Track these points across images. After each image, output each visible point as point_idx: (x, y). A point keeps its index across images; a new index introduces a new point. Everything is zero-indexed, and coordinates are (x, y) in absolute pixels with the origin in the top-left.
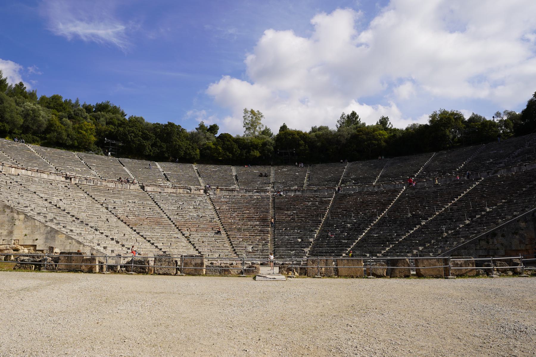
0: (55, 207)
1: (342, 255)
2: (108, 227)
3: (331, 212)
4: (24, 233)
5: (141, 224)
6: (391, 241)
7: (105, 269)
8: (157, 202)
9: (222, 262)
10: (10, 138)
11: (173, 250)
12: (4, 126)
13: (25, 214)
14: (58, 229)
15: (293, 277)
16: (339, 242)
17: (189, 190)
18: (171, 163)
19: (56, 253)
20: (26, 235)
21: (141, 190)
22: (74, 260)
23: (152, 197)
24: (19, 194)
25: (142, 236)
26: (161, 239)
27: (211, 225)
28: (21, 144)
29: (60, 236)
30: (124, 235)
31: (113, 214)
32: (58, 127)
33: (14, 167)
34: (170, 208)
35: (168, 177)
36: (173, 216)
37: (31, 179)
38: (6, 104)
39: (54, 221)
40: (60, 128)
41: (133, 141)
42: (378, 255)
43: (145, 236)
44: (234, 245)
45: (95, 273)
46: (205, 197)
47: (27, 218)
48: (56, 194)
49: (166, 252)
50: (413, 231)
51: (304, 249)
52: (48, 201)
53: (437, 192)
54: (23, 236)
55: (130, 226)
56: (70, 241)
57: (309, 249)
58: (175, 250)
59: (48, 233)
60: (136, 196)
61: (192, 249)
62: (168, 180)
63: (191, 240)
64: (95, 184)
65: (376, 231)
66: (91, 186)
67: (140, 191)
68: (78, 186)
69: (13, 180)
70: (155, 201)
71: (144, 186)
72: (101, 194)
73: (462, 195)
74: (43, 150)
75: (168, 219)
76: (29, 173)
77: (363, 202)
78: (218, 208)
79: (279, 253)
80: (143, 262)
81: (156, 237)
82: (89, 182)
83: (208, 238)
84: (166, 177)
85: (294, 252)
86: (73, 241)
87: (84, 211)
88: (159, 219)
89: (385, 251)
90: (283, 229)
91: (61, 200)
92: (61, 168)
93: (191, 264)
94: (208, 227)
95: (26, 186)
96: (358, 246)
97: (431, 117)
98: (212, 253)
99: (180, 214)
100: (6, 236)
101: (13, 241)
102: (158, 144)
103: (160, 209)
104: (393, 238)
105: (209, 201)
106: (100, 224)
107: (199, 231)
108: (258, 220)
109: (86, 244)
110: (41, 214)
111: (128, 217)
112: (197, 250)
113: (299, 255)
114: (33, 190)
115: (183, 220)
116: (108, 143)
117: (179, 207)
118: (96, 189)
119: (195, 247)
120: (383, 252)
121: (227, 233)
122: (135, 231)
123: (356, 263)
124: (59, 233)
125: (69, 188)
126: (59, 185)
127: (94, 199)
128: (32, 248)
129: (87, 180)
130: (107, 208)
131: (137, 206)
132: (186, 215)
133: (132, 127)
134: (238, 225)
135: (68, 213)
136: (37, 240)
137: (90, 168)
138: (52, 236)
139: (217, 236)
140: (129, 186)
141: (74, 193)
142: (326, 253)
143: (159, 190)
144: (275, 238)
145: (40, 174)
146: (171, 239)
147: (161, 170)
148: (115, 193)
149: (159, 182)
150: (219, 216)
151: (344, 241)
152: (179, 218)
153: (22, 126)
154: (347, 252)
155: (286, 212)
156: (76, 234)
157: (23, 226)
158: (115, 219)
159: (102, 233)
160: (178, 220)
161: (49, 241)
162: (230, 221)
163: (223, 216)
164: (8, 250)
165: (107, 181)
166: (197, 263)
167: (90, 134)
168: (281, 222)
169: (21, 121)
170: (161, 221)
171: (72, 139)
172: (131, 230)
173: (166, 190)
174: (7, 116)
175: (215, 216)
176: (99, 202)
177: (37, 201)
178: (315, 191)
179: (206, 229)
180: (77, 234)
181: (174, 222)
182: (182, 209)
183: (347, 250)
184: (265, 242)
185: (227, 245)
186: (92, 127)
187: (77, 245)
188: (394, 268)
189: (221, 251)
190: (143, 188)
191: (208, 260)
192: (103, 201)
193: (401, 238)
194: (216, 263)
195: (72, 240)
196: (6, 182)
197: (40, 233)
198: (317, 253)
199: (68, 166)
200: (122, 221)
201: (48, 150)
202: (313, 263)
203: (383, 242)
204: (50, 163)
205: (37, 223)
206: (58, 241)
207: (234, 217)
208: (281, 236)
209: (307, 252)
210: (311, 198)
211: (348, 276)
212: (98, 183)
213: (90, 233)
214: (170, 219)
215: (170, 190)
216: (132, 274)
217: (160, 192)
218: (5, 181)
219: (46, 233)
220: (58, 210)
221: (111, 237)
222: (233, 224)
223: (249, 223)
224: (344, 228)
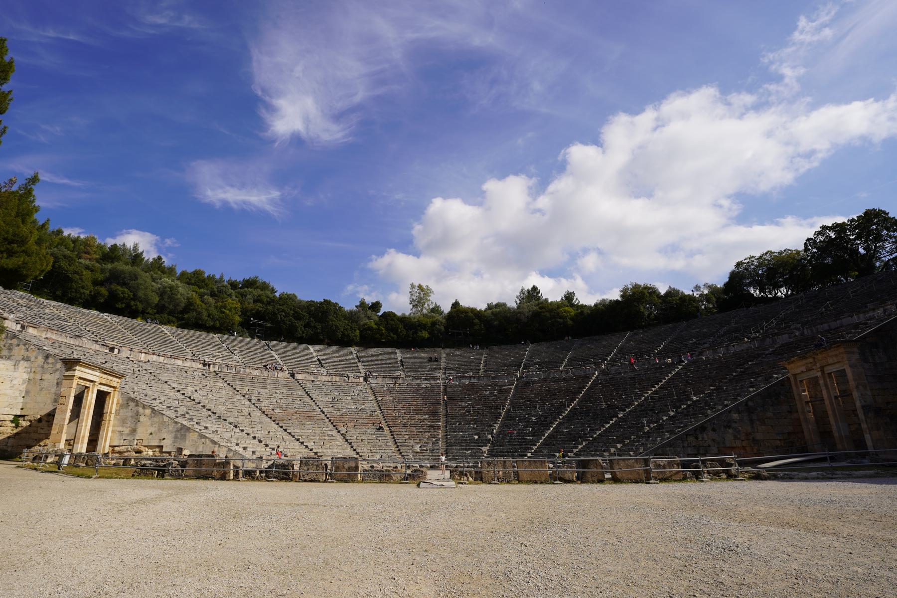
0: (189, 399)
2: (250, 423)
3: (512, 402)
4: (149, 431)
5: (290, 419)
6: (584, 437)
7: (240, 475)
8: (309, 393)
9: (384, 465)
10: (143, 319)
11: (326, 450)
12: (137, 305)
13: (152, 408)
14: (190, 427)
15: (465, 483)
18: (326, 346)
19: (185, 455)
20: (151, 434)
21: (291, 378)
22: (204, 464)
23: (303, 387)
24: (147, 384)
25: (290, 433)
26: (312, 438)
28: (154, 325)
30: (269, 432)
31: (257, 407)
32: (198, 305)
33: (144, 353)
34: (323, 399)
35: (323, 362)
36: (327, 409)
37: (163, 367)
39: (187, 416)
40: (200, 307)
41: (283, 321)
43: (293, 434)
45: (229, 480)
46: (365, 386)
47: (154, 413)
48: (191, 384)
50: (609, 425)
51: (482, 448)
52: (181, 392)
53: (634, 378)
54: (148, 435)
55: (277, 422)
56: (203, 440)
57: (488, 448)
58: (328, 450)
59: (178, 431)
60: (284, 386)
62: (322, 366)
63: (347, 438)
65: (566, 425)
68: (217, 374)
69: (142, 367)
70: (307, 391)
71: (294, 374)
72: (243, 384)
74: (179, 332)
75: (321, 413)
76: (161, 359)
77: (549, 391)
78: (380, 399)
79: (452, 453)
80: (287, 466)
81: (307, 434)
83: (368, 435)
84: (320, 362)
85: (469, 452)
86: (207, 440)
89: (577, 450)
91: (196, 391)
93: (344, 467)
95: (155, 374)
96: (546, 444)
98: (373, 454)
99: (336, 407)
100: (128, 435)
101: (136, 441)
103: (312, 401)
104: (586, 434)
105: (369, 391)
106: (241, 419)
107: (358, 427)
108: (427, 413)
109: (222, 444)
110: (172, 408)
111: (275, 411)
112: (355, 450)
113: (476, 456)
114: (164, 379)
115: (339, 414)
117: (335, 398)
118: (237, 377)
119: (352, 447)
120: (575, 451)
121: (390, 429)
122: (282, 427)
123: (539, 465)
125: (206, 377)
126: (195, 373)
127: (235, 389)
128: (157, 450)
129: (228, 366)
130: (250, 400)
131: (286, 398)
132: (342, 407)
133: (283, 305)
135: (204, 406)
136: (164, 439)
137: (233, 353)
140: (276, 374)
141: (212, 382)
142: (507, 452)
144: (447, 435)
146: (324, 437)
147: (315, 354)
148: (261, 382)
149: (312, 369)
150: (382, 408)
151: (528, 438)
153: (157, 305)
154: (533, 451)
155: (460, 403)
156: (211, 432)
157: (149, 423)
158: (259, 413)
159: (242, 431)
161: (179, 440)
162: (394, 414)
163: (386, 408)
164: (129, 452)
166: (351, 467)
167: (234, 314)
169: (156, 299)
170: (312, 415)
172: (276, 426)
173: (320, 378)
175: (377, 408)
176: (240, 393)
177: (167, 392)
178: (494, 378)
179: (365, 425)
180: (213, 431)
181: (328, 416)
182: (337, 400)
183: (532, 449)
184: (436, 440)
185: (391, 443)
187: (211, 445)
188: (584, 471)
189: (383, 451)
190: (293, 375)
191: (368, 463)
192: (245, 392)
193: (596, 433)
196: (134, 370)
197: (168, 431)
198: (497, 452)
199: (207, 351)
200: (267, 415)
201: (185, 332)
202: (489, 465)
203: (574, 438)
204: (186, 347)
205: (166, 419)
208: (454, 432)
209: (485, 452)
210: (489, 386)
211: (531, 481)
213: (228, 430)
214: (324, 413)
215: (324, 378)
216: (272, 481)
217: (313, 381)
218: (132, 369)
219: (176, 431)
220: (192, 403)
223: (417, 416)
224: (528, 421)
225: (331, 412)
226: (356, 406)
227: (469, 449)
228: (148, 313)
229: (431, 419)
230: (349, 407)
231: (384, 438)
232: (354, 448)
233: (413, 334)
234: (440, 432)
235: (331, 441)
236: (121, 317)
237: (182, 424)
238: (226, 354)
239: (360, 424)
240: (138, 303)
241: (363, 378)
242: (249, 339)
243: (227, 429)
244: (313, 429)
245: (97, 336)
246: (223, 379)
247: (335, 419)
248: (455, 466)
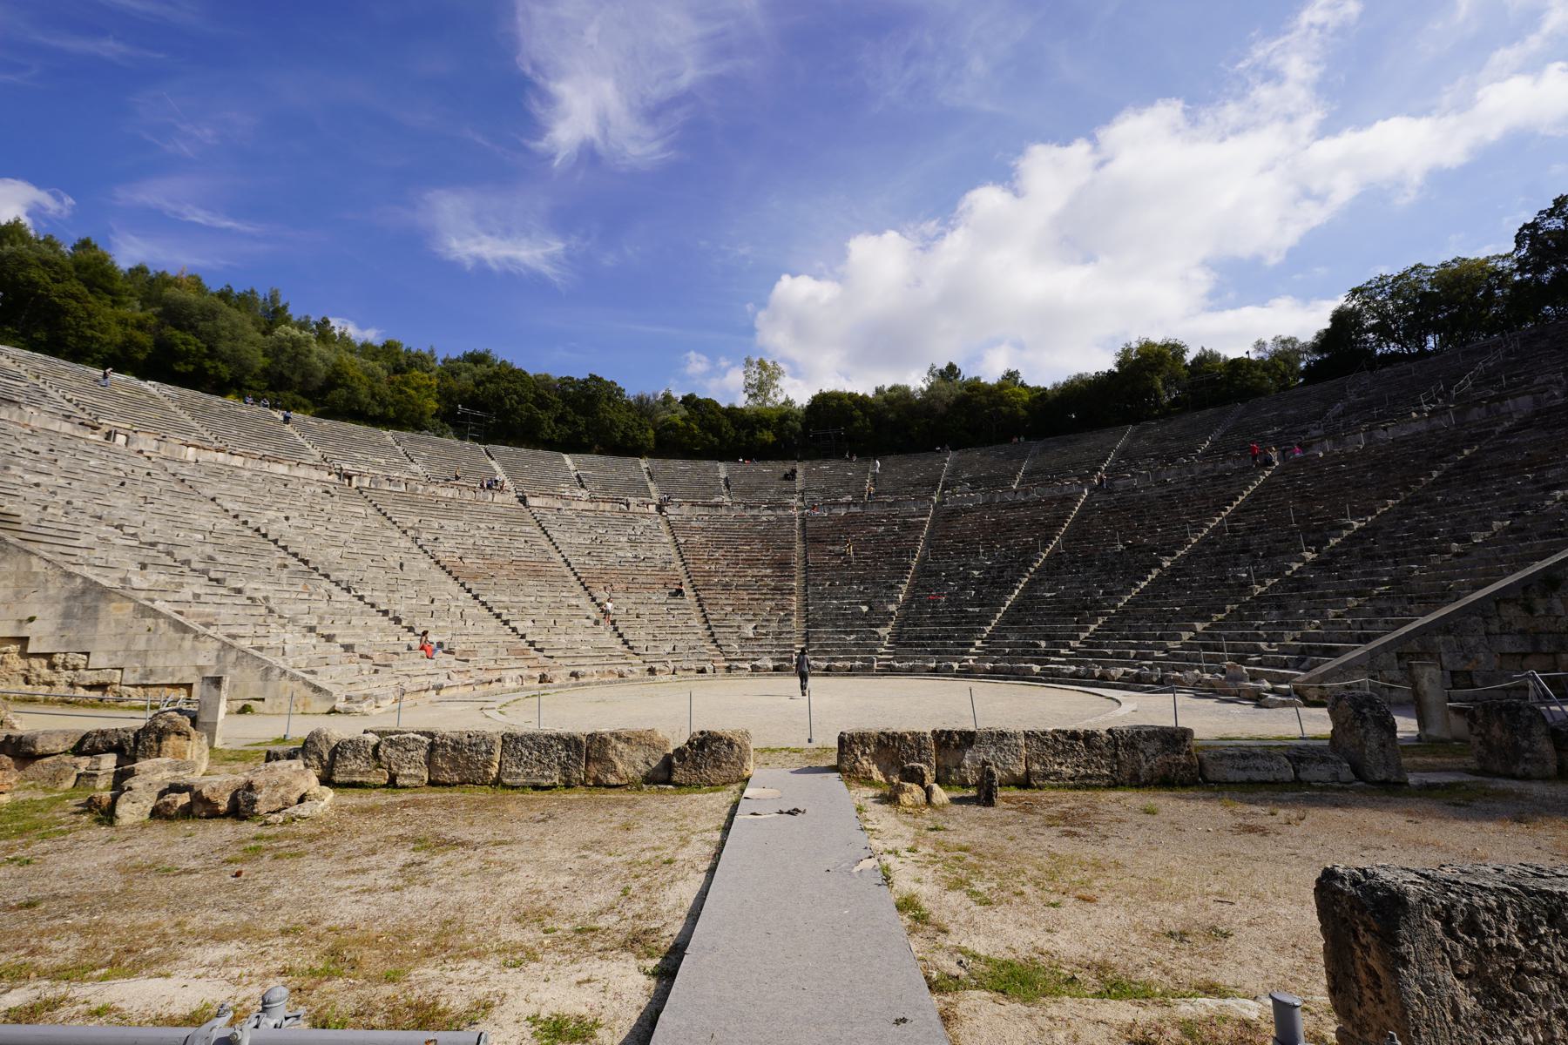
1: (974, 644)
3: (929, 544)
6: (1096, 608)
9: (678, 665)
10: (238, 397)
11: (558, 637)
12: (216, 368)
16: (961, 611)
18: (595, 456)
25: (484, 604)
26: (532, 611)
28: (261, 408)
29: (115, 608)
30: (432, 602)
31: (426, 552)
32: (352, 378)
33: (192, 446)
34: (572, 540)
35: (585, 480)
36: (576, 557)
38: (221, 322)
40: (356, 380)
41: (516, 410)
42: (1072, 643)
43: (490, 605)
44: (711, 623)
46: (657, 518)
49: (534, 642)
51: (878, 630)
52: (242, 519)
53: (1170, 496)
57: (889, 629)
58: (562, 637)
59: (73, 597)
60: (498, 516)
61: (608, 634)
65: (1047, 585)
68: (361, 492)
73: (1241, 498)
75: (565, 565)
76: (238, 461)
77: (997, 524)
78: (682, 541)
79: (819, 639)
81: (523, 605)
82: (395, 486)
83: (653, 606)
84: (580, 481)
85: (853, 637)
86: (161, 621)
87: (341, 544)
88: (540, 564)
89: (1087, 634)
90: (824, 585)
96: (1011, 620)
97: (1119, 354)
98: (657, 643)
102: (570, 418)
104: (1097, 601)
105: (664, 528)
107: (634, 590)
108: (770, 566)
110: (160, 547)
112: (620, 635)
113: (867, 645)
114: (209, 492)
116: (464, 415)
119: (616, 629)
120: (1083, 635)
121: (697, 595)
122: (469, 591)
124: (114, 596)
127: (390, 519)
129: (391, 481)
130: (415, 540)
133: (515, 382)
136: (31, 619)
137: (412, 461)
138: (89, 608)
139: (674, 601)
140: (490, 496)
142: (931, 638)
144: (807, 605)
145: (267, 463)
146: (558, 611)
147: (572, 467)
148: (451, 509)
151: (971, 610)
152: (591, 562)
153: (264, 370)
154: (985, 635)
155: (831, 548)
158: (424, 563)
161: (77, 622)
167: (426, 397)
168: (820, 569)
169: (261, 362)
170: (544, 569)
171: (382, 403)
173: (574, 505)
174: (224, 346)
178: (890, 505)
179: (648, 586)
181: (576, 570)
183: (983, 631)
184: (786, 615)
185: (697, 622)
186: (429, 383)
187: (172, 633)
189: (678, 637)
190: (523, 500)
191: (644, 662)
192: (410, 525)
194: (663, 668)
195: (155, 618)
197: (46, 598)
198: (909, 638)
199: (356, 455)
200: (444, 568)
203: (1080, 610)
205: (37, 565)
206: (108, 624)
208: (821, 599)
209: (885, 637)
212: (417, 489)
214: (569, 565)
215: (582, 505)
217: (559, 509)
219: (67, 599)
221: (383, 608)
223: (750, 571)
224: (965, 578)
225: (585, 564)
226: (634, 553)
227: (852, 633)
228: (250, 388)
229: (777, 576)
230: (620, 553)
231: (684, 611)
232: (620, 631)
233: (747, 437)
234: (795, 598)
235: (572, 618)
236: (185, 391)
237: (85, 579)
238: (396, 460)
239: (637, 586)
240: (219, 364)
242: (455, 442)
243: (310, 595)
245: (83, 409)
246: (371, 501)
247: (590, 575)
248: (824, 667)
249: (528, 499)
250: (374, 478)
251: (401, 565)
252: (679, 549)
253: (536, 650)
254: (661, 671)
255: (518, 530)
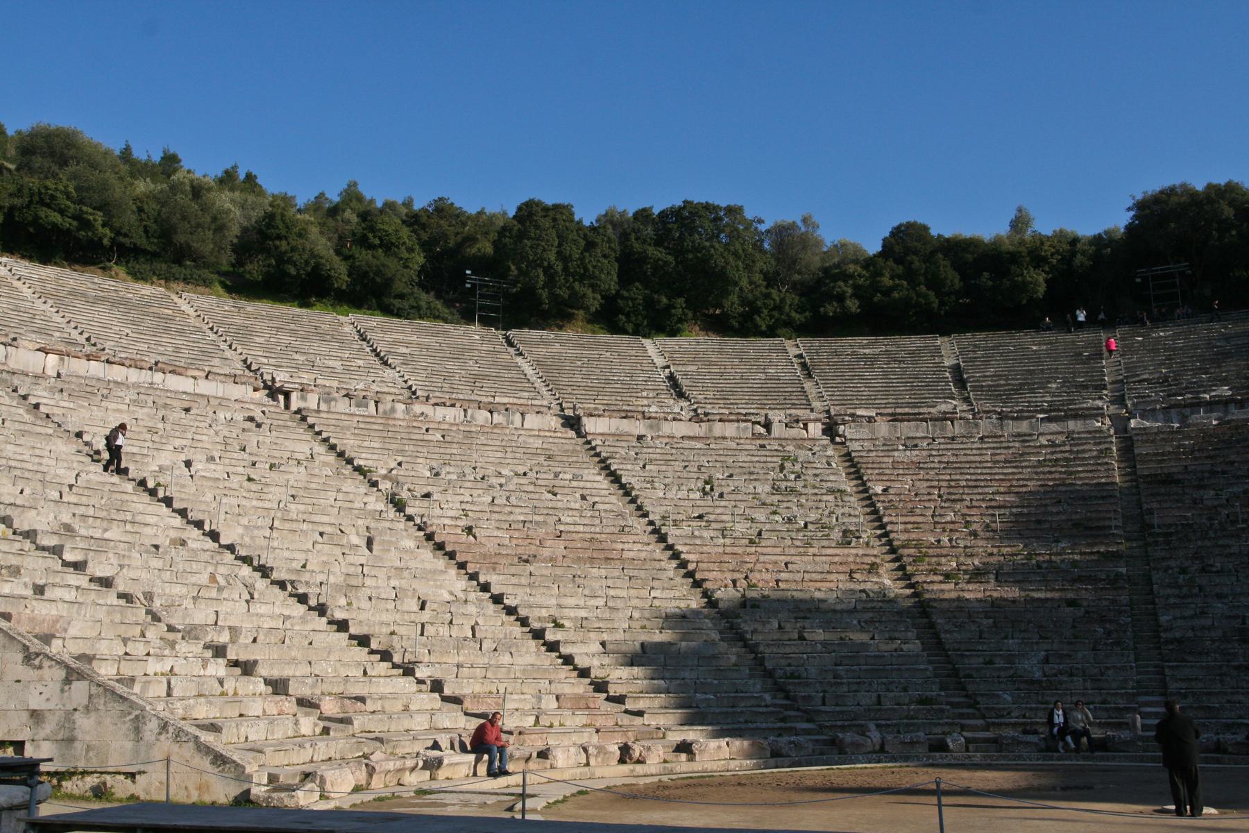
17: (764, 426)
25: (511, 611)
27: (844, 560)
30: (422, 608)
43: (523, 612)
46: (825, 447)
62: (681, 395)
64: (385, 412)
66: (356, 419)
67: (559, 435)
72: (387, 446)
78: (879, 489)
82: (358, 406)
92: (265, 361)
94: (833, 568)
122: (485, 588)
134: (972, 555)
137: (385, 363)
143: (639, 427)
149: (645, 402)
150: (885, 520)
158: (409, 540)
160: (698, 542)
165: (432, 401)
173: (667, 428)
182: (721, 495)
199: (297, 356)
200: (440, 547)
201: (249, 309)
207: (952, 522)
212: (393, 410)
217: (640, 438)
221: (339, 615)
222: (944, 551)
225: (693, 536)
238: (360, 363)
241: (819, 426)
244: (612, 592)
249: (585, 420)
250: (327, 398)
251: (370, 543)
252: (873, 505)
253: (608, 699)
254: (857, 745)
255: (569, 476)
